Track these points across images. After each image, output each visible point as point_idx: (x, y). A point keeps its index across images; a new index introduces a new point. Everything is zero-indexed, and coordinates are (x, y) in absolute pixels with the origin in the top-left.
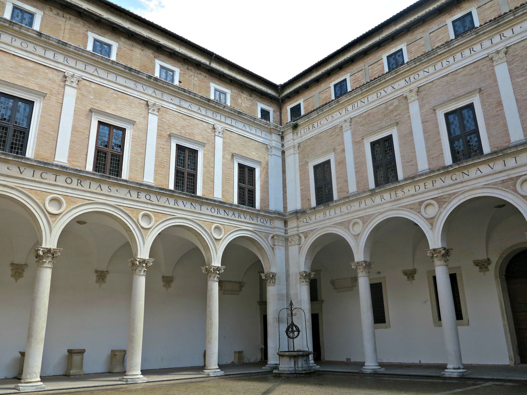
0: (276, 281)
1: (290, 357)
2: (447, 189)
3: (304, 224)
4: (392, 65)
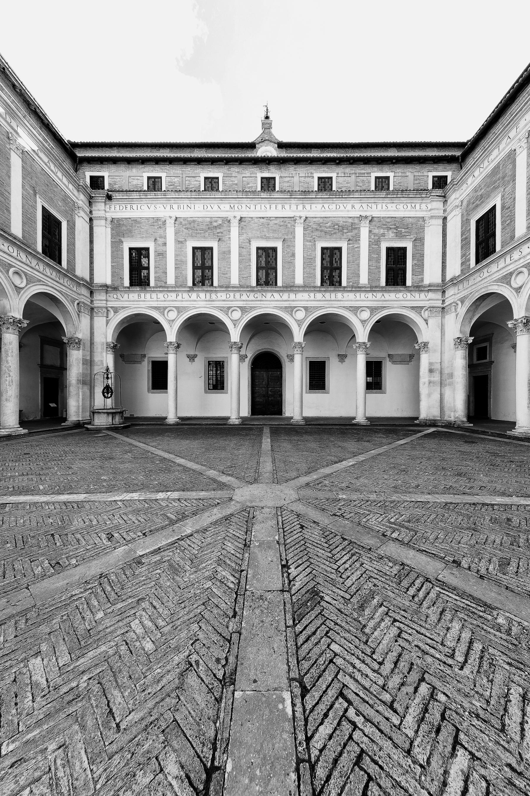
0: (81, 346)
1: (108, 413)
2: (250, 303)
3: (113, 299)
4: (208, 187)
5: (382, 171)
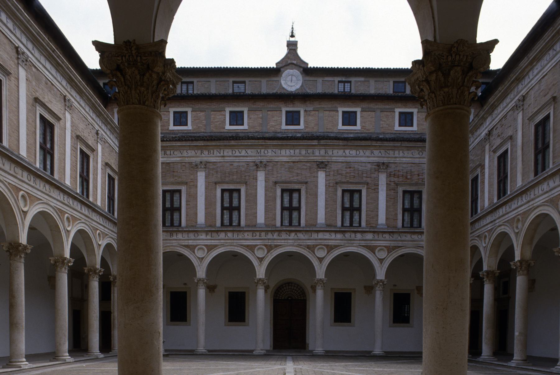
5: (406, 107)
